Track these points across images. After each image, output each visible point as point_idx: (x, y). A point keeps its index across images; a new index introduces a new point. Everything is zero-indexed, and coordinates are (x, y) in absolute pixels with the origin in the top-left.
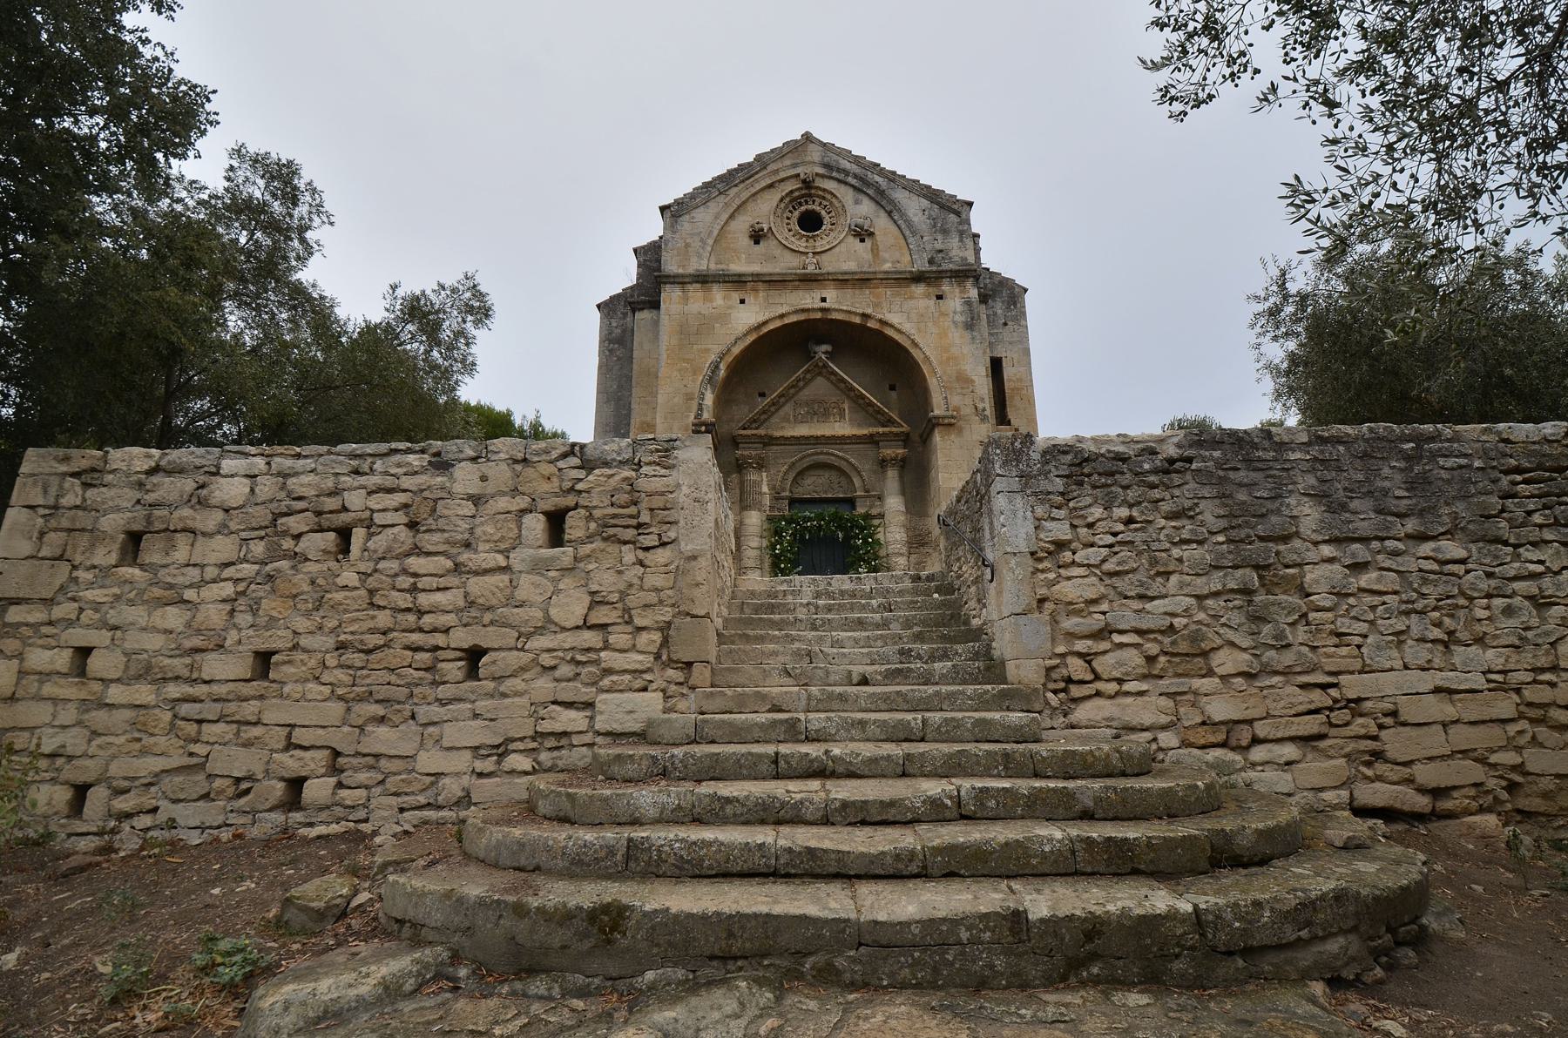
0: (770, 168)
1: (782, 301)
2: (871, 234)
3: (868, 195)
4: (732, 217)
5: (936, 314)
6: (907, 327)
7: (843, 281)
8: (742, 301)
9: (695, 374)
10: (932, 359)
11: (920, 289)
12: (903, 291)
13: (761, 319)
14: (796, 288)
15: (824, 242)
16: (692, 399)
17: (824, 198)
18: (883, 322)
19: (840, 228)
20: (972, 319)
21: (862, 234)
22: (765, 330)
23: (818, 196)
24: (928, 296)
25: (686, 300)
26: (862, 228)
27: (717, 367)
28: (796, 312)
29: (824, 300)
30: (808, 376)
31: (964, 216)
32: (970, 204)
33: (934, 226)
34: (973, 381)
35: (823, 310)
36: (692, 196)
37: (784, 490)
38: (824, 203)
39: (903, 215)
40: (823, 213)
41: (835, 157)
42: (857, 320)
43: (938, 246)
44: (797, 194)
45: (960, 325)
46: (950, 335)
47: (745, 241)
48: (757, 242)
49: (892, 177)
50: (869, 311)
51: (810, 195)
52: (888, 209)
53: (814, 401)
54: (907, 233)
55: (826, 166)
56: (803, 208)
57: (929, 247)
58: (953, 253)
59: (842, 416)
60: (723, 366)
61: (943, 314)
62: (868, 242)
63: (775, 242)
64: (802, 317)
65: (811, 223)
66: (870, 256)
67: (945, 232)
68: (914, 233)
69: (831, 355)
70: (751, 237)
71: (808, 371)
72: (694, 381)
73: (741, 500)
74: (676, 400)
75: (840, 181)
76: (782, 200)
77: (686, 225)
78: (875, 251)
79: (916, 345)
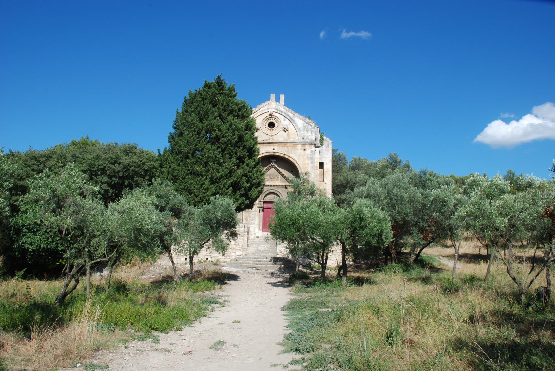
0: (261, 110)
2: (288, 130)
6: (296, 158)
7: (279, 144)
11: (299, 147)
12: (295, 147)
14: (267, 146)
15: (275, 132)
21: (285, 130)
24: (301, 149)
28: (266, 153)
29: (274, 149)
30: (270, 168)
33: (305, 129)
37: (262, 199)
38: (276, 120)
39: (296, 125)
41: (279, 107)
42: (282, 155)
44: (268, 117)
46: (306, 161)
51: (272, 118)
53: (271, 175)
55: (276, 109)
56: (270, 121)
59: (278, 179)
61: (305, 155)
64: (268, 154)
65: (272, 125)
66: (286, 137)
67: (307, 131)
69: (275, 163)
71: (269, 167)
75: (280, 114)
78: (288, 135)
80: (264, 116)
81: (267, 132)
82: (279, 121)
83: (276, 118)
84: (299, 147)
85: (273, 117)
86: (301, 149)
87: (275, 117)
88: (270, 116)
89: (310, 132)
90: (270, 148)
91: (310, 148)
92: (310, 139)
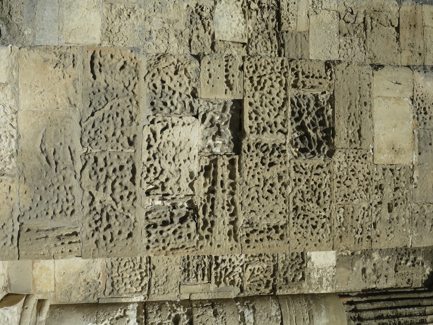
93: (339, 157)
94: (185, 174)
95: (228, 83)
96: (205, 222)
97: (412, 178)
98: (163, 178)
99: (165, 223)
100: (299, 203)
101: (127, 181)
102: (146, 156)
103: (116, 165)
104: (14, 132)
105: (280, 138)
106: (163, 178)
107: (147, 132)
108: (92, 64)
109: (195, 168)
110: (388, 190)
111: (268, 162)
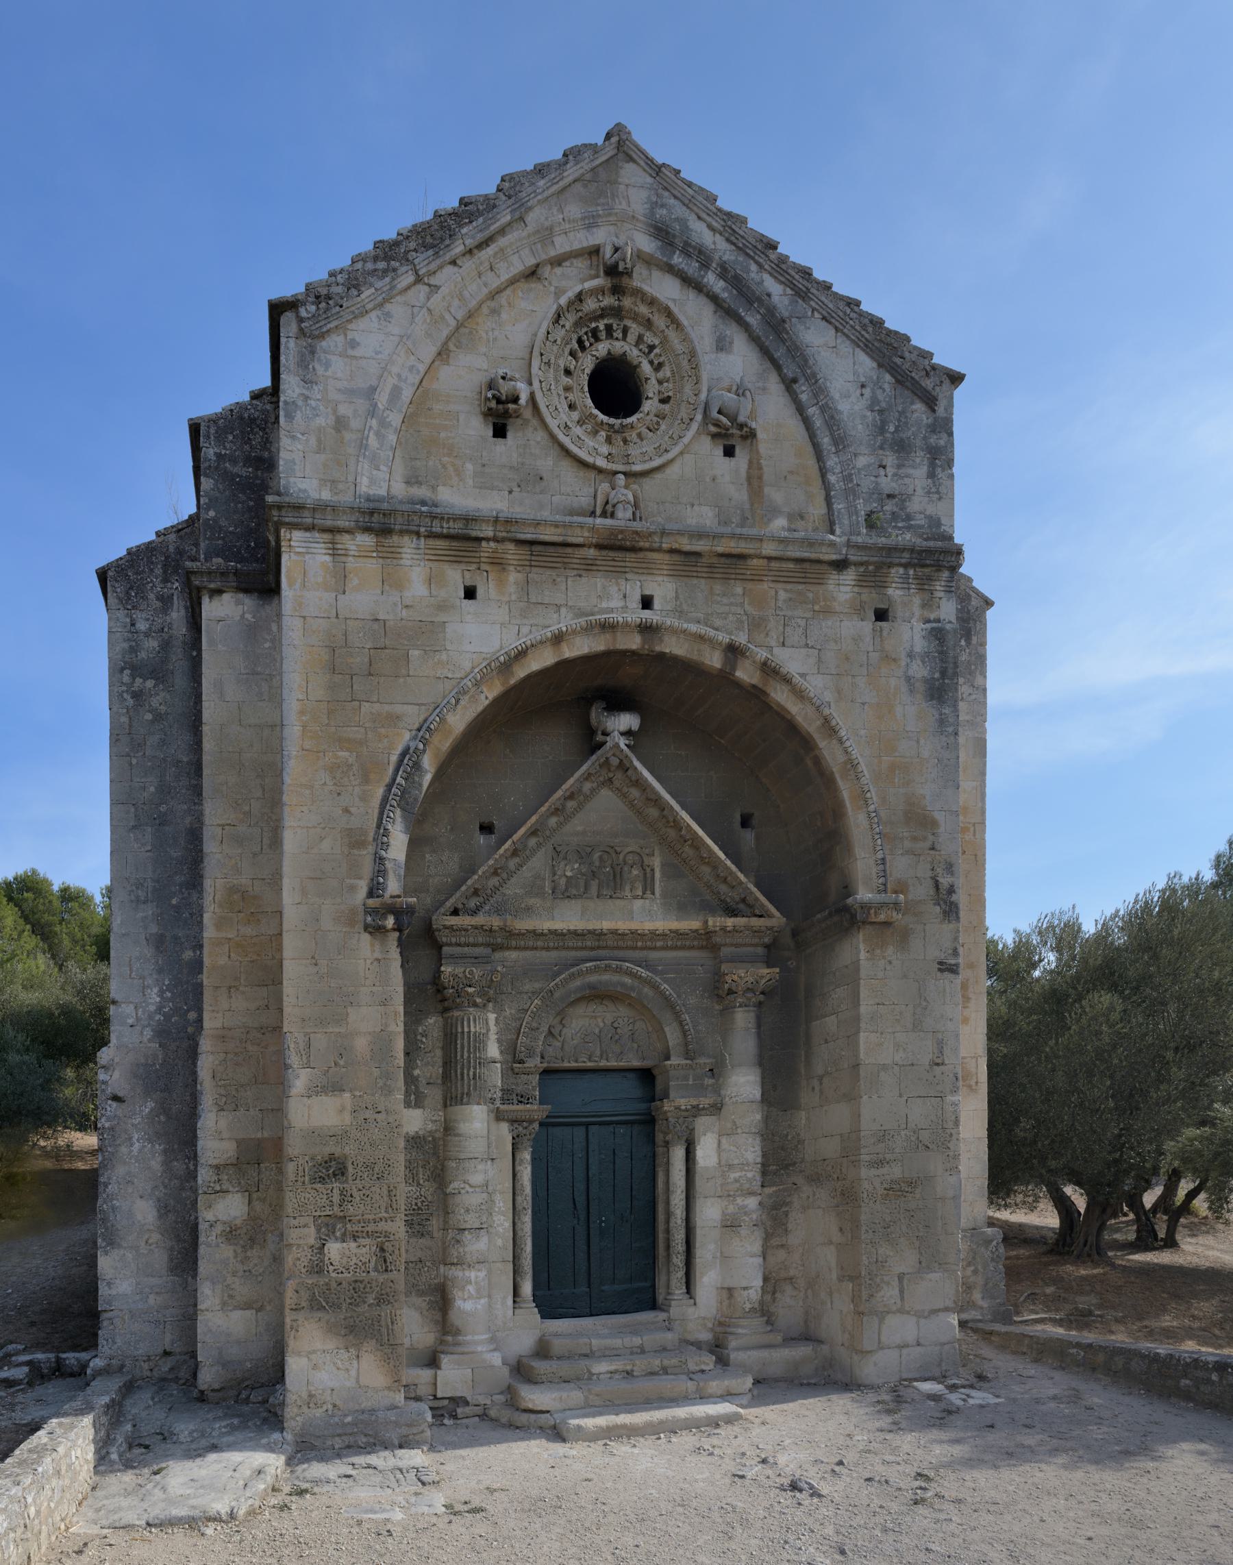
1: (559, 598)
3: (745, 326)
4: (443, 354)
5: (875, 656)
8: (470, 593)
9: (366, 780)
10: (863, 767)
13: (513, 642)
14: (589, 567)
15: (647, 447)
16: (360, 844)
17: (648, 324)
18: (769, 670)
19: (684, 413)
20: (943, 673)
22: (521, 672)
23: (635, 317)
24: (858, 610)
25: (340, 580)
26: (733, 419)
27: (417, 766)
31: (940, 411)
32: (956, 378)
33: (882, 429)
34: (934, 824)
35: (646, 629)
36: (353, 279)
39: (819, 391)
40: (646, 368)
42: (715, 660)
43: (887, 484)
44: (591, 305)
45: (920, 687)
47: (479, 428)
48: (500, 432)
49: (801, 283)
50: (741, 639)
51: (617, 312)
52: (790, 371)
54: (825, 441)
57: (866, 483)
58: (915, 506)
60: (429, 764)
61: (889, 659)
62: (742, 459)
63: (540, 435)
67: (902, 447)
68: (840, 442)
70: (488, 413)
72: (364, 798)
73: (446, 1077)
74: (326, 846)
75: (687, 281)
76: (558, 318)
77: (338, 366)
78: (754, 480)
79: (830, 729)
80: (558, 293)
81: (590, 442)
82: (678, 347)
83: (660, 321)
84: (843, 588)
85: (627, 302)
86: (858, 610)
87: (643, 309)
88: (609, 301)
89: (920, 457)
90: (613, 589)
91: (924, 606)
92: (920, 521)
93: (347, 1150)
94: (358, 1251)
95: (304, 1227)
96: (385, 1237)
97: (360, 1096)
98: (360, 1264)
99: (385, 1261)
100: (375, 1177)
101: (362, 1286)
102: (346, 1275)
103: (352, 1292)
104: (335, 1351)
105: (336, 1192)
106: (360, 1264)
107: (334, 1275)
108: (296, 1309)
109: (353, 1245)
110: (367, 1115)
111: (350, 1199)
